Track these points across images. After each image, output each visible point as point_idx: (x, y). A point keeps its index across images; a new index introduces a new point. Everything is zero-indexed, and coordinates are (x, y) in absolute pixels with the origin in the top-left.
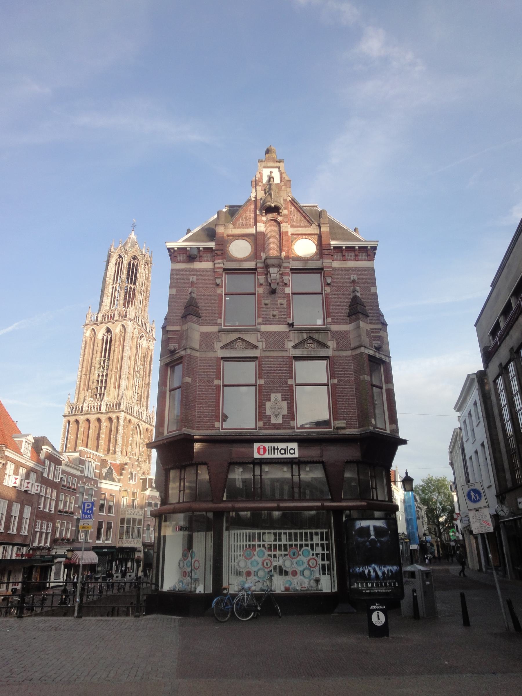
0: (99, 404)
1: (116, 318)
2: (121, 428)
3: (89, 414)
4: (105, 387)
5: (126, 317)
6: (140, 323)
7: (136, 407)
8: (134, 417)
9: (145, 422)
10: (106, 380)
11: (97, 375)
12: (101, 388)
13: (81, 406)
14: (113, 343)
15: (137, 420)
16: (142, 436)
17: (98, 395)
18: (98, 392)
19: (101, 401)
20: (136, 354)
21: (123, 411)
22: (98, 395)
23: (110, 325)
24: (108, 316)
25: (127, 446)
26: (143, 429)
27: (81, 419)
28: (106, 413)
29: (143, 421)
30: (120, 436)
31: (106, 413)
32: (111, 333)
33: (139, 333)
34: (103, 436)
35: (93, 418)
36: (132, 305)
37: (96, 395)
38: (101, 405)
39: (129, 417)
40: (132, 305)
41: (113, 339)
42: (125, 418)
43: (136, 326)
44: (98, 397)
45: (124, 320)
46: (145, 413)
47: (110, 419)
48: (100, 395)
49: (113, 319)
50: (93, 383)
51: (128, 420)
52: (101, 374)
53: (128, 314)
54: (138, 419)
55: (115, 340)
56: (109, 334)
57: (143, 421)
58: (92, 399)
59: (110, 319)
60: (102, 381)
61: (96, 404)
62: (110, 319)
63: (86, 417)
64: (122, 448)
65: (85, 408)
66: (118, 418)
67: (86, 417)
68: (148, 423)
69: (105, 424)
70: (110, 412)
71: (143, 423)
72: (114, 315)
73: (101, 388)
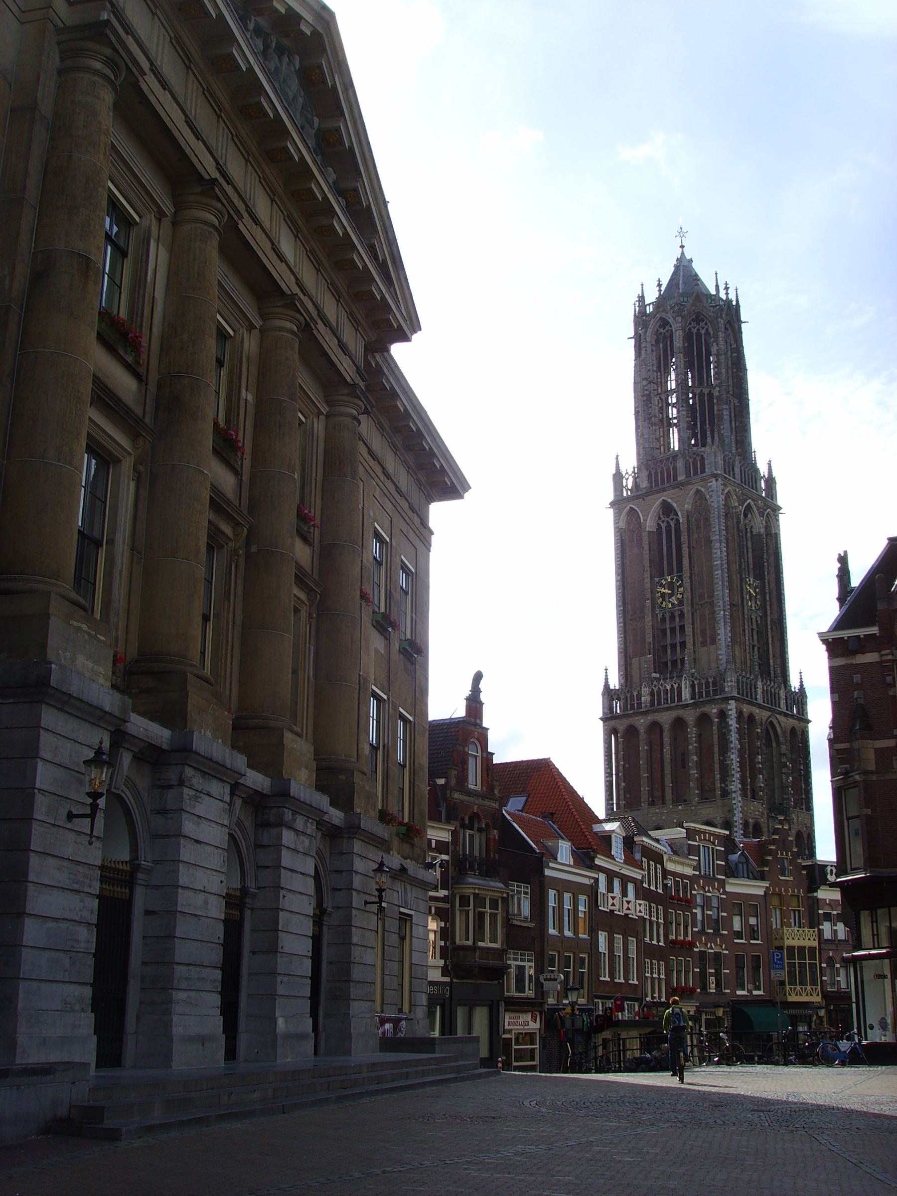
0: (676, 686)
1: (681, 478)
2: (734, 737)
4: (683, 645)
5: (703, 471)
6: (738, 476)
7: (759, 684)
8: (760, 706)
9: (786, 715)
10: (682, 628)
11: (660, 616)
12: (673, 646)
13: (635, 694)
14: (684, 538)
15: (766, 714)
16: (783, 748)
17: (669, 664)
20: (741, 556)
21: (733, 698)
22: (669, 664)
23: (669, 496)
24: (662, 473)
25: (753, 777)
26: (784, 732)
27: (641, 723)
28: (695, 705)
29: (780, 713)
30: (734, 758)
31: (695, 705)
33: (741, 502)
34: (695, 758)
35: (666, 718)
36: (713, 438)
37: (666, 664)
38: (680, 687)
39: (746, 709)
40: (713, 438)
41: (683, 527)
42: (740, 713)
44: (670, 668)
45: (702, 480)
46: (782, 694)
47: (704, 719)
48: (674, 662)
51: (746, 715)
52: (667, 616)
53: (706, 462)
54: (769, 710)
57: (780, 713)
58: (658, 675)
60: (673, 630)
61: (668, 688)
63: (650, 718)
64: (743, 781)
66: (723, 715)
67: (650, 718)
68: (792, 716)
69: (692, 732)
70: (705, 703)
71: (782, 718)
72: (675, 469)
73: (673, 646)
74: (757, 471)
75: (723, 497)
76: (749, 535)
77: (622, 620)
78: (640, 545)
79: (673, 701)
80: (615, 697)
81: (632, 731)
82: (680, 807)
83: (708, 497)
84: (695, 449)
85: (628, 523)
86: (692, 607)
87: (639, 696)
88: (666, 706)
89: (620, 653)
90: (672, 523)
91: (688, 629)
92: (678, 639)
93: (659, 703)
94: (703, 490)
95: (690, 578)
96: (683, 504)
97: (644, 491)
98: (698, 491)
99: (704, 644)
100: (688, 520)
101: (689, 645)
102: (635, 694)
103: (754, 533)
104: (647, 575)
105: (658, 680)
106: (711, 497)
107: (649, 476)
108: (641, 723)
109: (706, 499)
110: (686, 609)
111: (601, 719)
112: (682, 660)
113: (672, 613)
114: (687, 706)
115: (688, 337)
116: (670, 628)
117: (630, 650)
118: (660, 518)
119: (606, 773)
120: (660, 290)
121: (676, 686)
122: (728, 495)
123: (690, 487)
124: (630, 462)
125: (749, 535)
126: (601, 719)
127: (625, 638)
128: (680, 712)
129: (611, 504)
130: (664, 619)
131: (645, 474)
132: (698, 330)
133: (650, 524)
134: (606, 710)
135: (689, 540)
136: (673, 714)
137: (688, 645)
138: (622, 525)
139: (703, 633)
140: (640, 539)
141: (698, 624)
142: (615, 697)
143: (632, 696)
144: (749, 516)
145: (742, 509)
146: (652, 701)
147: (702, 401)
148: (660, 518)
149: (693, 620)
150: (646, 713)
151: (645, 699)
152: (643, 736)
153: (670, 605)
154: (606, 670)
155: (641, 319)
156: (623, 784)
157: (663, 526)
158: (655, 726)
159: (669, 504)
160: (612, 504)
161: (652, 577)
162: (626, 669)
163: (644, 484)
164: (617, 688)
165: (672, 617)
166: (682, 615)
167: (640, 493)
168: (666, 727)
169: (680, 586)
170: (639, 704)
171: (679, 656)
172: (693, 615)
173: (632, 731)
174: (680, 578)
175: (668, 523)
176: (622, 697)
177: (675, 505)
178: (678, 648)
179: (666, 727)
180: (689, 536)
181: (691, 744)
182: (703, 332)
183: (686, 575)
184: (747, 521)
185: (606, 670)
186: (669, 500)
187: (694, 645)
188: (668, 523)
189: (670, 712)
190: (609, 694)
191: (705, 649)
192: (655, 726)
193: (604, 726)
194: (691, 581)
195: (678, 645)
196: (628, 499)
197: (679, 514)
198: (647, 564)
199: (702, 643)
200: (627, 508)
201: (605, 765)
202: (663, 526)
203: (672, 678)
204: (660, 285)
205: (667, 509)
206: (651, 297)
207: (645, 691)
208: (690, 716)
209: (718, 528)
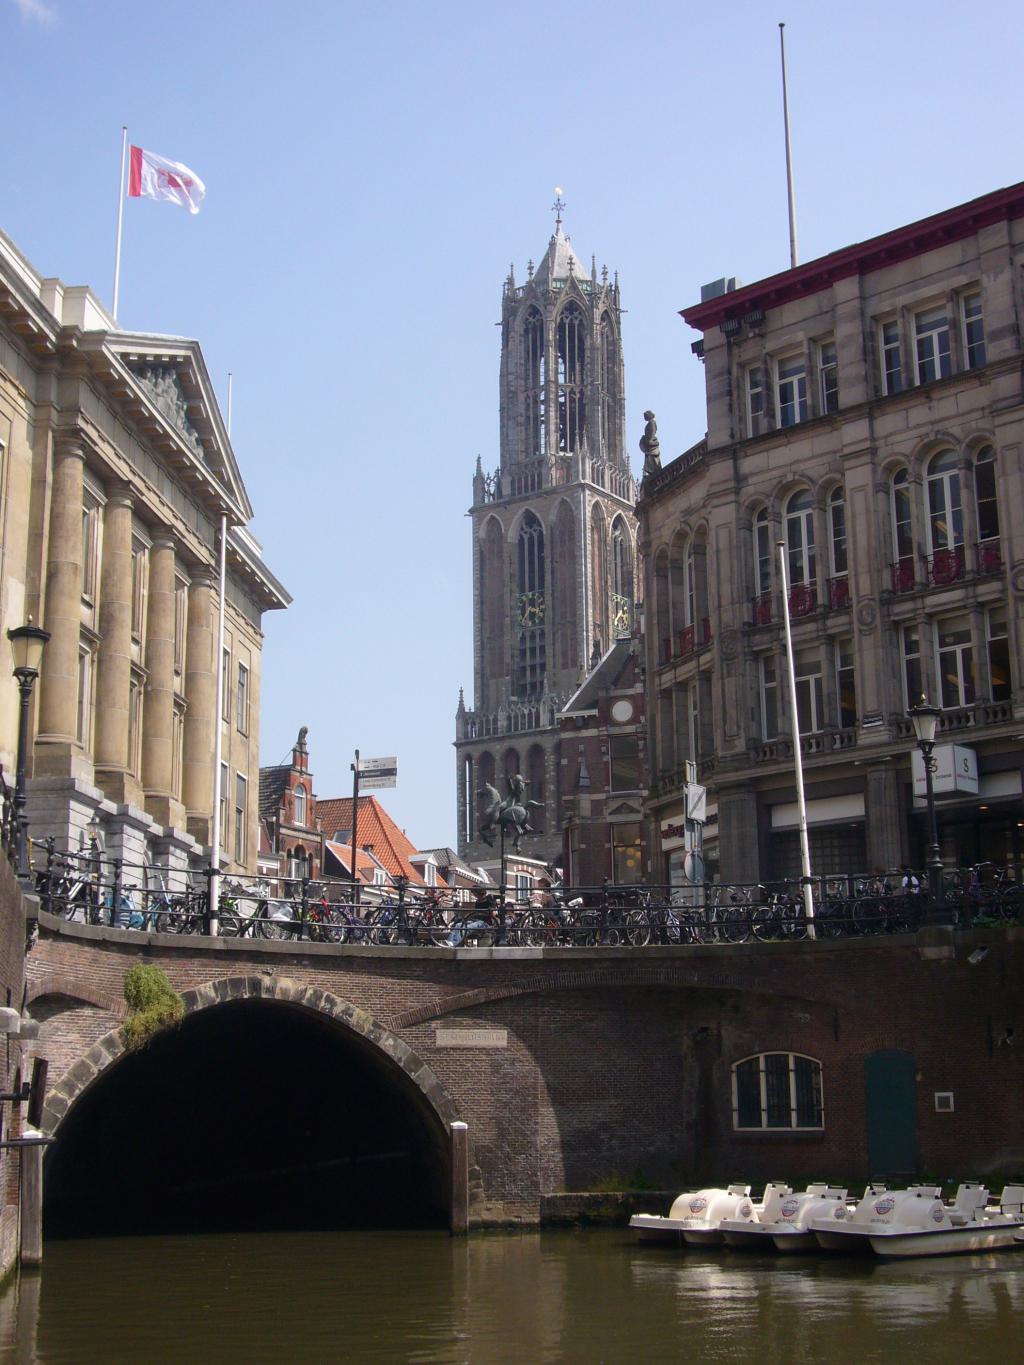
0: (534, 711)
3: (514, 737)
4: (543, 666)
10: (542, 648)
11: (520, 635)
12: (533, 668)
13: (491, 718)
14: (547, 552)
17: (528, 687)
18: (528, 679)
19: (538, 701)
22: (528, 687)
23: (532, 506)
27: (497, 749)
32: (540, 526)
34: (552, 787)
35: (523, 745)
36: (581, 444)
37: (524, 687)
40: (581, 444)
41: (547, 541)
43: (597, 498)
44: (528, 692)
49: (540, 487)
50: (512, 657)
52: (528, 634)
55: (552, 542)
56: (535, 527)
58: (514, 699)
59: (533, 489)
60: (533, 650)
61: (526, 712)
62: (533, 489)
63: (507, 744)
65: (502, 723)
67: (507, 744)
69: (550, 759)
72: (540, 475)
74: (629, 478)
75: (589, 509)
76: (618, 548)
77: (479, 638)
78: (500, 557)
79: (530, 727)
80: (470, 721)
81: (486, 758)
82: (535, 839)
83: (573, 508)
84: (562, 454)
85: (489, 532)
86: (554, 625)
87: (495, 721)
88: (523, 732)
89: (476, 673)
90: (535, 535)
91: (549, 651)
92: (538, 660)
93: (516, 729)
94: (568, 500)
95: (552, 595)
96: (549, 517)
97: (507, 499)
98: (563, 502)
99: (565, 666)
100: (552, 533)
101: (549, 666)
102: (491, 718)
103: (624, 546)
104: (507, 590)
105: (516, 703)
106: (577, 508)
107: (512, 483)
108: (497, 749)
109: (571, 510)
110: (547, 628)
111: (455, 744)
112: (542, 683)
113: (533, 632)
114: (545, 732)
115: (561, 328)
116: (530, 648)
117: (488, 671)
118: (522, 529)
119: (459, 802)
120: (531, 274)
121: (534, 711)
122: (596, 506)
123: (555, 496)
124: (492, 465)
125: (618, 548)
126: (455, 744)
127: (482, 657)
128: (538, 739)
129: (470, 511)
130: (523, 639)
131: (506, 481)
132: (571, 320)
133: (511, 535)
134: (460, 735)
135: (552, 554)
136: (531, 740)
137: (548, 667)
138: (482, 534)
139: (564, 654)
140: (500, 552)
141: (558, 646)
142: (470, 721)
143: (488, 721)
144: (619, 527)
145: (610, 521)
146: (509, 725)
147: (572, 401)
148: (522, 529)
149: (554, 639)
150: (502, 739)
151: (502, 723)
152: (498, 764)
153: (530, 624)
154: (461, 691)
155: (510, 305)
156: (477, 814)
157: (526, 537)
158: (511, 753)
159: (533, 514)
160: (472, 511)
161: (511, 591)
162: (483, 691)
163: (506, 491)
164: (473, 711)
165: (533, 637)
166: (542, 635)
167: (502, 500)
168: (523, 754)
169: (542, 603)
170: (495, 730)
171: (538, 678)
172: (554, 634)
173: (486, 758)
174: (542, 594)
175: (531, 534)
176: (477, 721)
177: (538, 515)
178: (538, 671)
179: (523, 754)
180: (552, 549)
181: (547, 773)
182: (576, 323)
183: (548, 591)
184: (617, 533)
185: (461, 691)
186: (533, 510)
187: (554, 667)
188: (531, 534)
189: (527, 738)
190: (463, 716)
191: (565, 671)
192: (511, 753)
193: (458, 752)
194: (553, 599)
195: (538, 666)
196: (490, 507)
197: (543, 525)
198: (507, 579)
199: (563, 665)
200: (488, 517)
201: (458, 793)
202: (526, 537)
203: (530, 702)
204: (531, 268)
205: (531, 520)
206: (521, 280)
207: (502, 716)
208: (548, 743)
209: (588, 540)
